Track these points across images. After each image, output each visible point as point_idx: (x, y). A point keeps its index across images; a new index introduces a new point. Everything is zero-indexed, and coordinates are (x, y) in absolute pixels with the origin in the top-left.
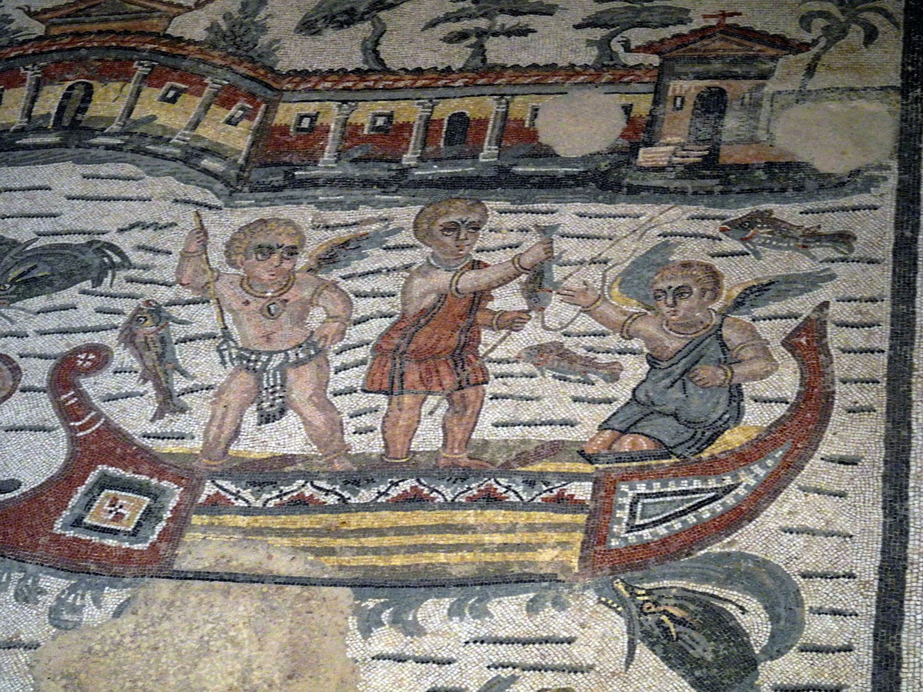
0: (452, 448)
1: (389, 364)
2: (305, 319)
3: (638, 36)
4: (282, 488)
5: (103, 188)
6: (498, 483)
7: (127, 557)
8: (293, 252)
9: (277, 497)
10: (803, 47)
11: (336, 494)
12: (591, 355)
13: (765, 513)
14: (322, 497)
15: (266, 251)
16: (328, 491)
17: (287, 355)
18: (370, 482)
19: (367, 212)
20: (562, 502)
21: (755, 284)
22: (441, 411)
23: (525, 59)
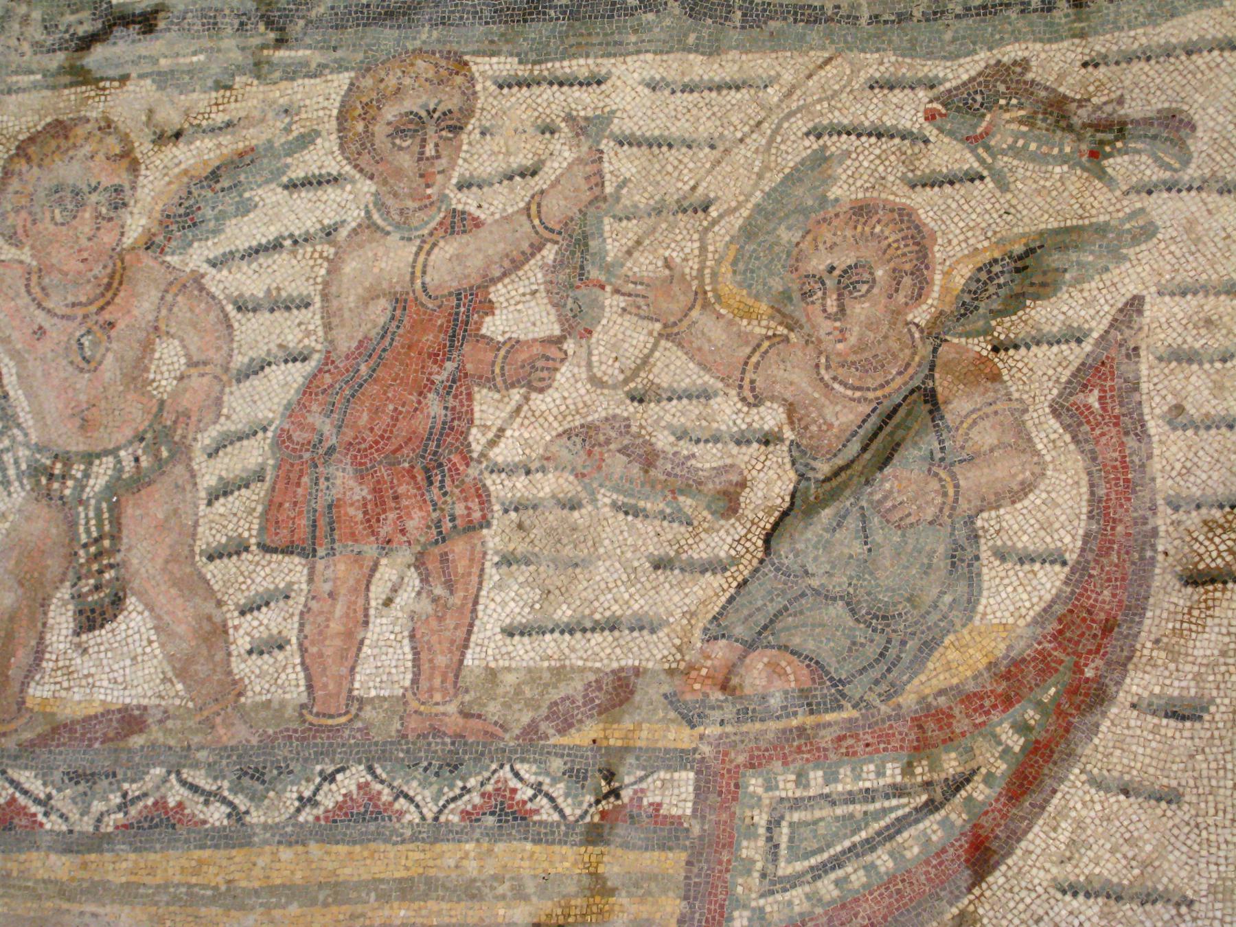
0: (431, 690)
1: (305, 479)
2: (147, 370)
4: (126, 786)
6: (517, 775)
9: (120, 808)
11: (224, 801)
12: (685, 448)
13: (1023, 844)
14: (196, 807)
16: (210, 794)
17: (117, 457)
18: (284, 771)
21: (997, 255)
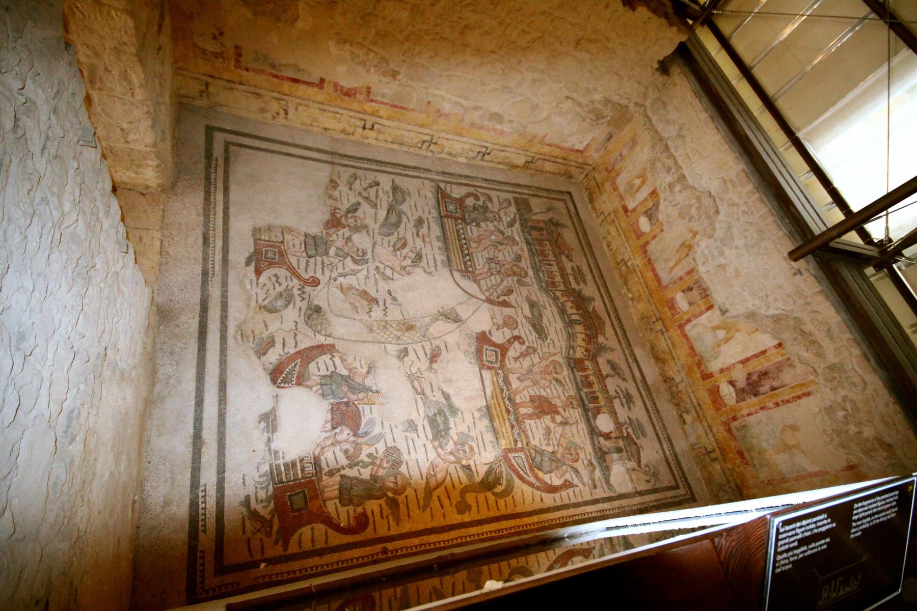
3: (630, 430)
5: (560, 334)
7: (482, 360)
8: (557, 373)
10: (640, 466)
15: (555, 368)
19: (570, 385)
20: (516, 441)
22: (529, 412)
23: (616, 407)
